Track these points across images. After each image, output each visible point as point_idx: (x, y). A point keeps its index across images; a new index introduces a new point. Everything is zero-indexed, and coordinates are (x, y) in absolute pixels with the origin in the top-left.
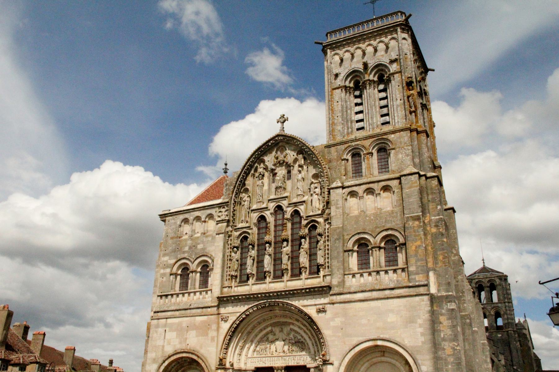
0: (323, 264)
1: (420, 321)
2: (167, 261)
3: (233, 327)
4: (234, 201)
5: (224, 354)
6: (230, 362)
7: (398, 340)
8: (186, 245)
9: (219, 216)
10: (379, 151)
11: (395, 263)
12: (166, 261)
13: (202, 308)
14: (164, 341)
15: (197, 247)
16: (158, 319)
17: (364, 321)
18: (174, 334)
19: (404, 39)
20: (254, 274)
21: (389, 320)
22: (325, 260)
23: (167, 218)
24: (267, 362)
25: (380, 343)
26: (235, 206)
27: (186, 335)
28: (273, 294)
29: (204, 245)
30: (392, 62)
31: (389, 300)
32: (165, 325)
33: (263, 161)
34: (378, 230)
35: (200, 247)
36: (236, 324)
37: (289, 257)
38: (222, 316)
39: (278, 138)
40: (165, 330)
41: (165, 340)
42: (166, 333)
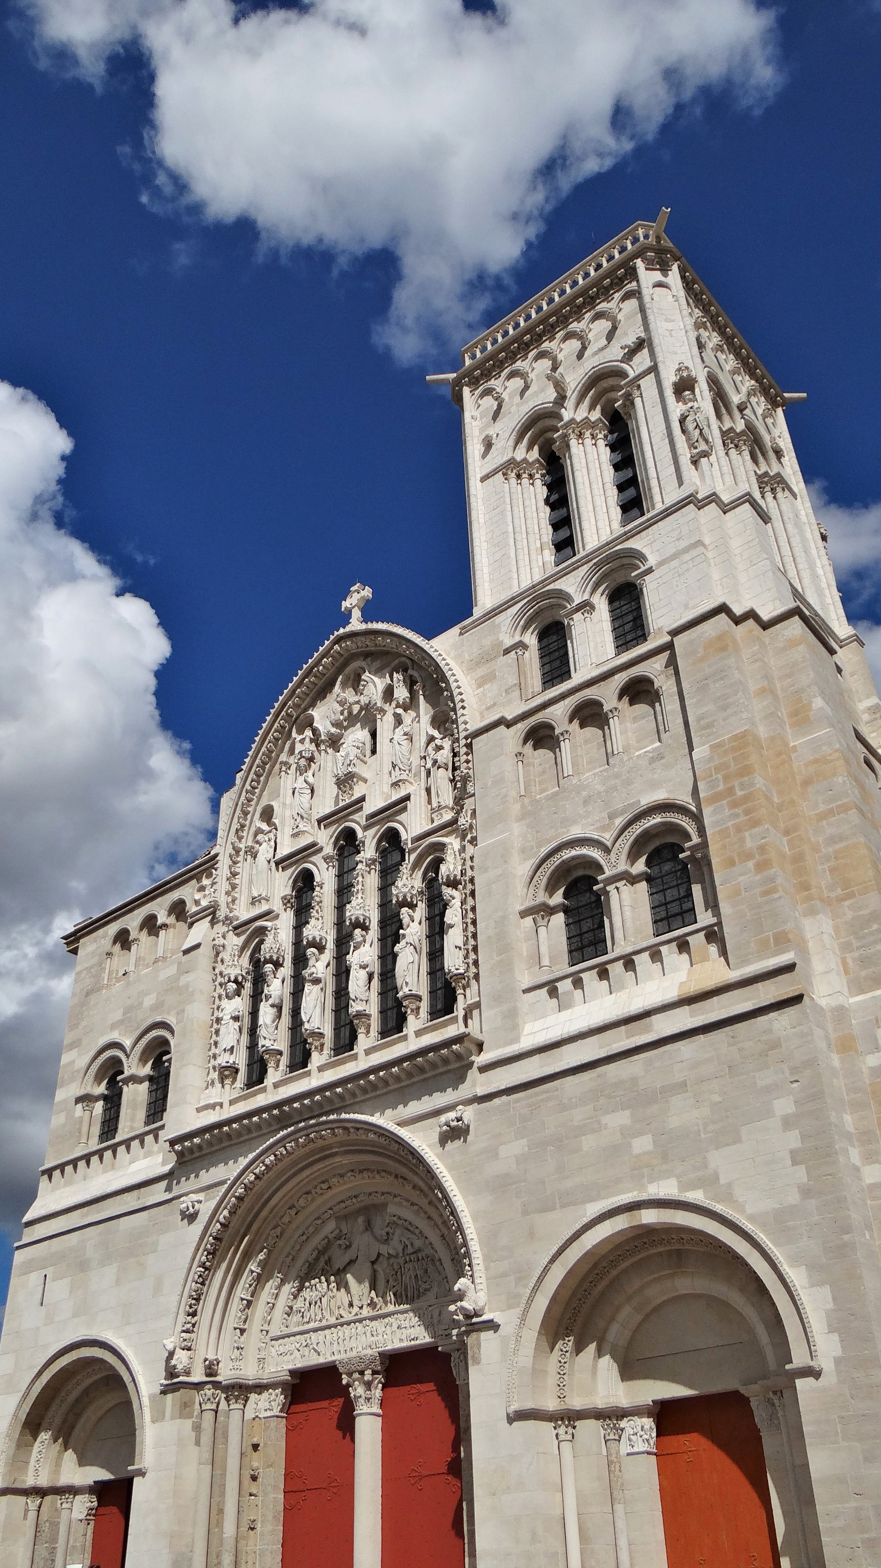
0: (461, 971)
3: (210, 1236)
4: (234, 848)
5: (184, 1335)
6: (206, 1360)
9: (197, 902)
10: (613, 598)
11: (688, 917)
19: (659, 285)
20: (280, 1053)
21: (674, 1122)
22: (466, 957)
24: (320, 1348)
25: (649, 1217)
26: (235, 863)
28: (312, 1101)
30: (632, 352)
33: (310, 723)
34: (619, 822)
36: (218, 1221)
37: (371, 976)
39: (340, 646)
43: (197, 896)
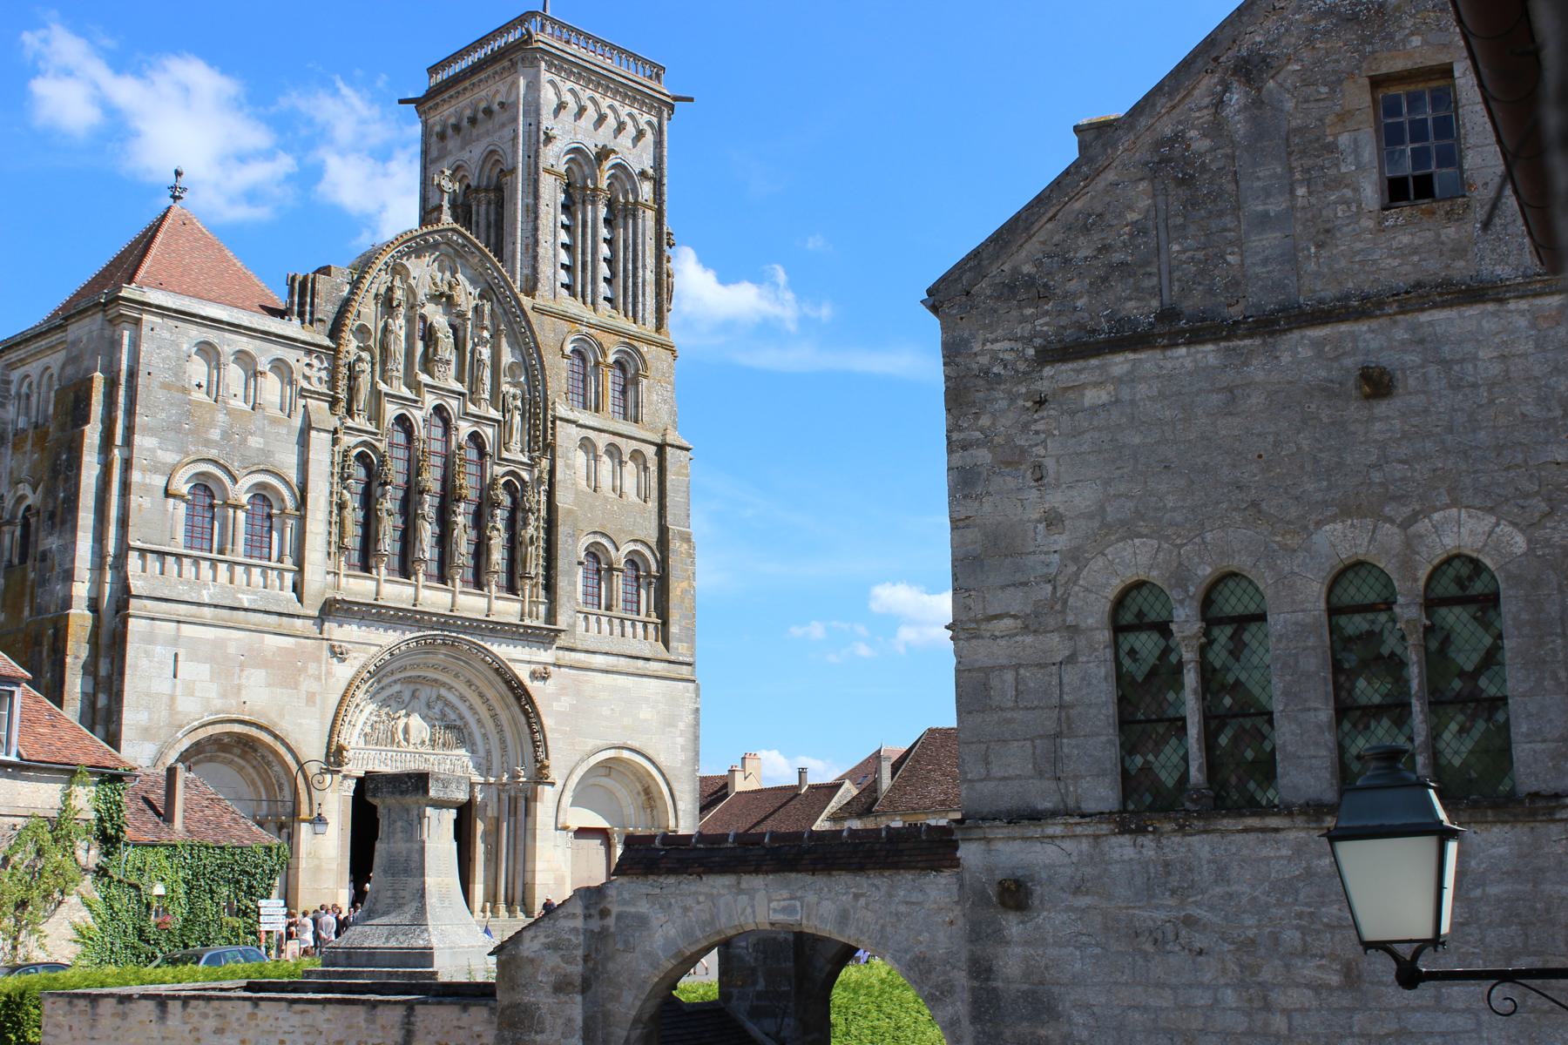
1: (681, 726)
2: (152, 451)
7: (650, 753)
8: (212, 424)
12: (148, 449)
13: (280, 614)
14: (175, 686)
15: (245, 440)
16: (153, 619)
17: (606, 711)
18: (204, 669)
21: (642, 716)
23: (145, 317)
25: (626, 754)
27: (240, 677)
29: (266, 443)
31: (644, 679)
32: (176, 640)
35: (255, 442)
38: (332, 647)
40: (176, 655)
41: (177, 681)
42: (179, 663)
43: (307, 371)
